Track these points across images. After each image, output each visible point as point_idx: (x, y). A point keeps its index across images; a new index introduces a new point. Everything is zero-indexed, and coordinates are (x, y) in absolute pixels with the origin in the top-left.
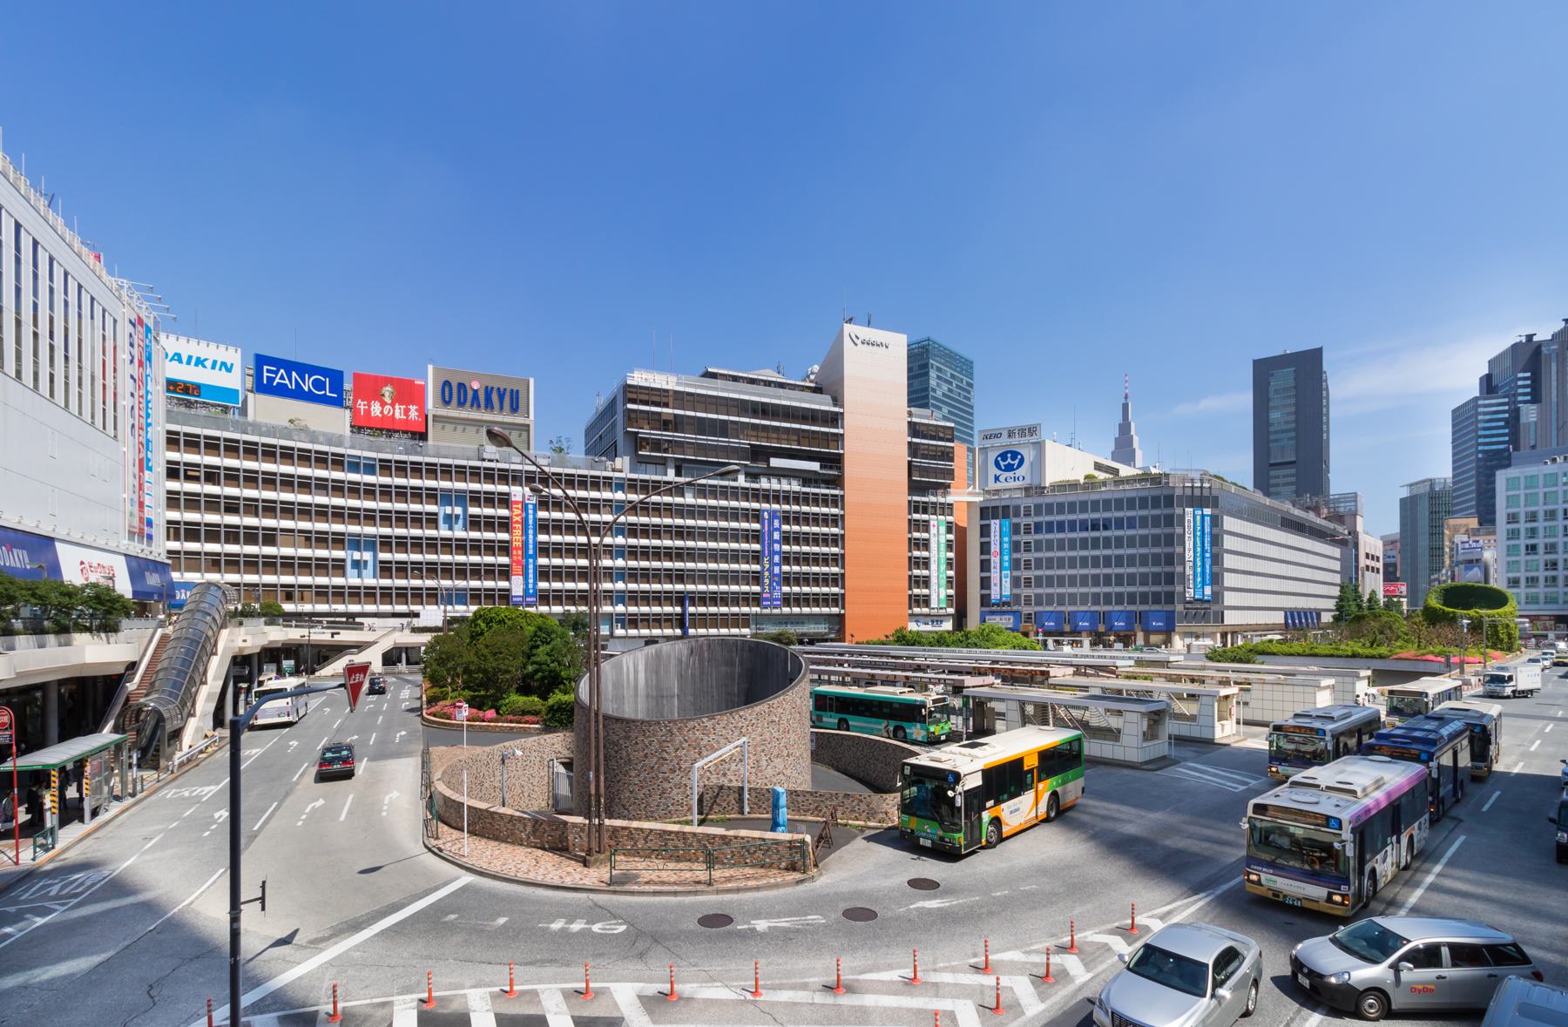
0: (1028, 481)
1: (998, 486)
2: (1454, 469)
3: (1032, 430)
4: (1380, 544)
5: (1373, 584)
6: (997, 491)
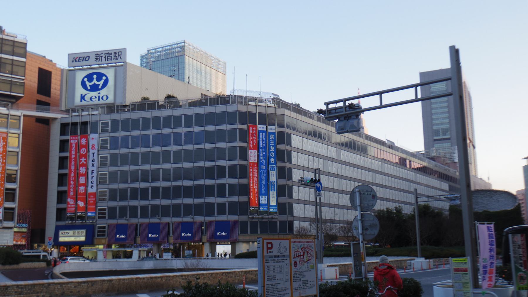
0: (111, 100)
3: (117, 55)
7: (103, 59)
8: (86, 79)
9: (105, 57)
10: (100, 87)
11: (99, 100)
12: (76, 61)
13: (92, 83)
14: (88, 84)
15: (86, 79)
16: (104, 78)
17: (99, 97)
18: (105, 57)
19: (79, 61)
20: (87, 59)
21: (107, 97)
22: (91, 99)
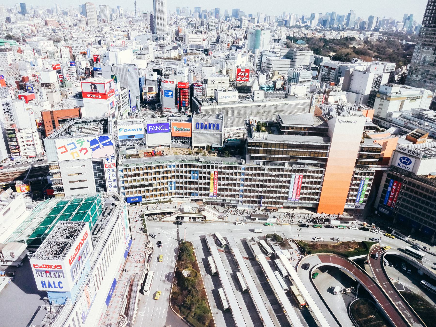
0: (410, 170)
1: (399, 166)
14: (402, 160)
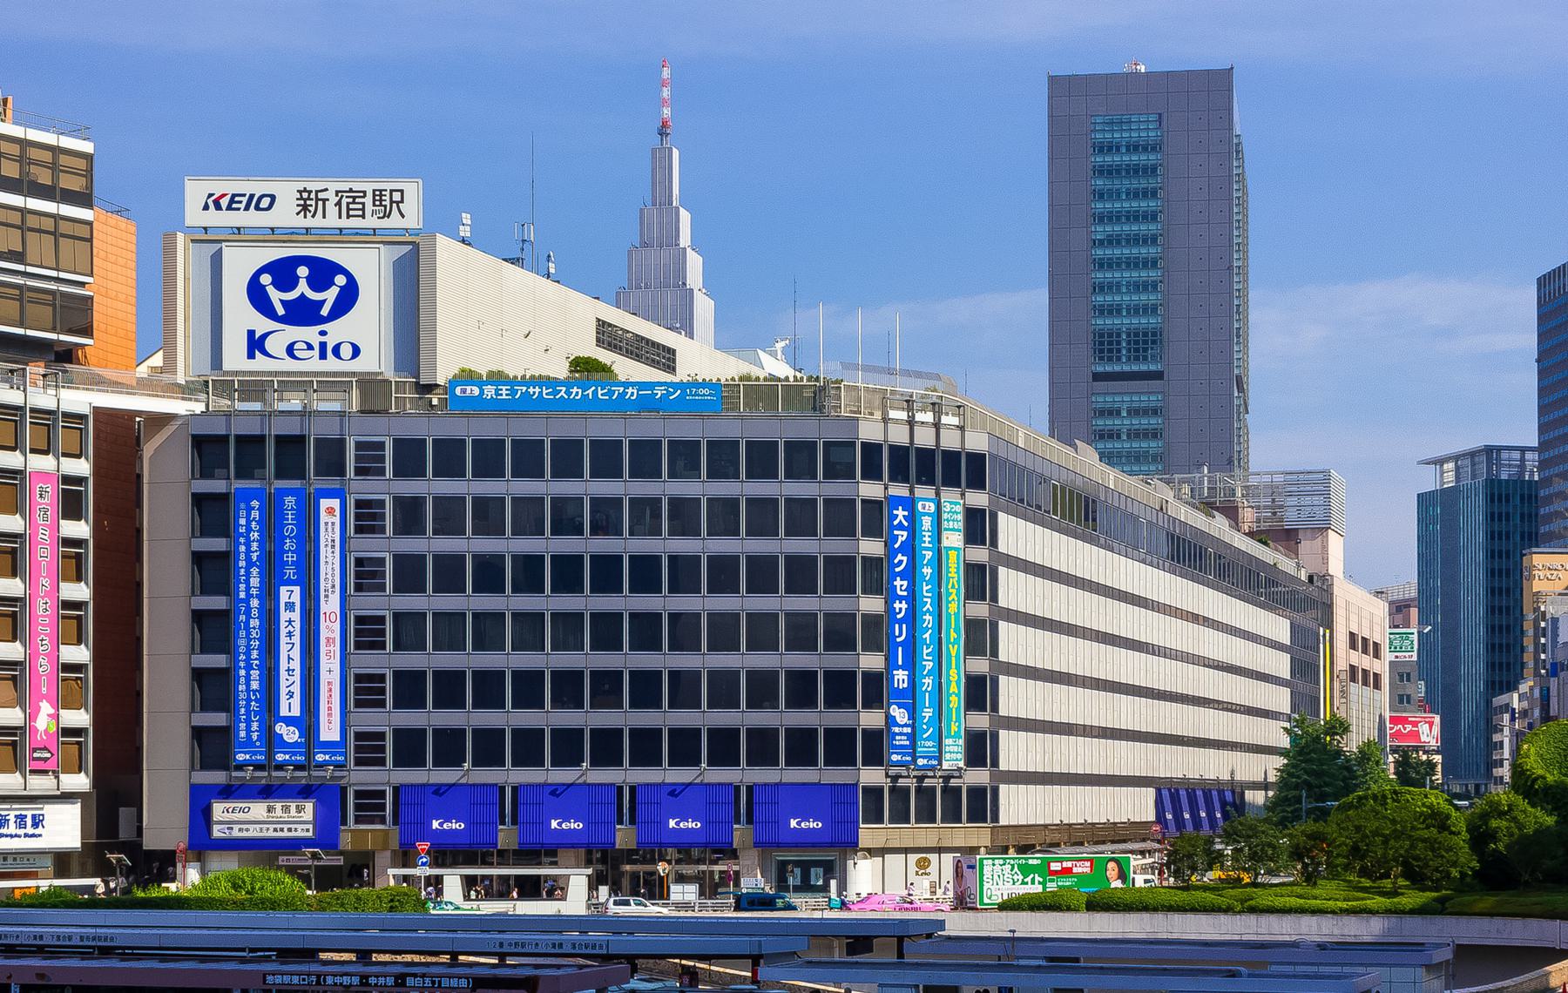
0: (367, 363)
2: (1543, 429)
4: (1380, 609)
5: (1365, 716)
6: (254, 388)
7: (332, 209)
8: (266, 279)
9: (339, 204)
10: (325, 312)
11: (323, 356)
12: (218, 207)
13: (292, 295)
14: (276, 296)
15: (266, 279)
16: (340, 280)
17: (323, 346)
18: (339, 204)
19: (229, 208)
20: (265, 203)
21: (356, 351)
22: (290, 350)
